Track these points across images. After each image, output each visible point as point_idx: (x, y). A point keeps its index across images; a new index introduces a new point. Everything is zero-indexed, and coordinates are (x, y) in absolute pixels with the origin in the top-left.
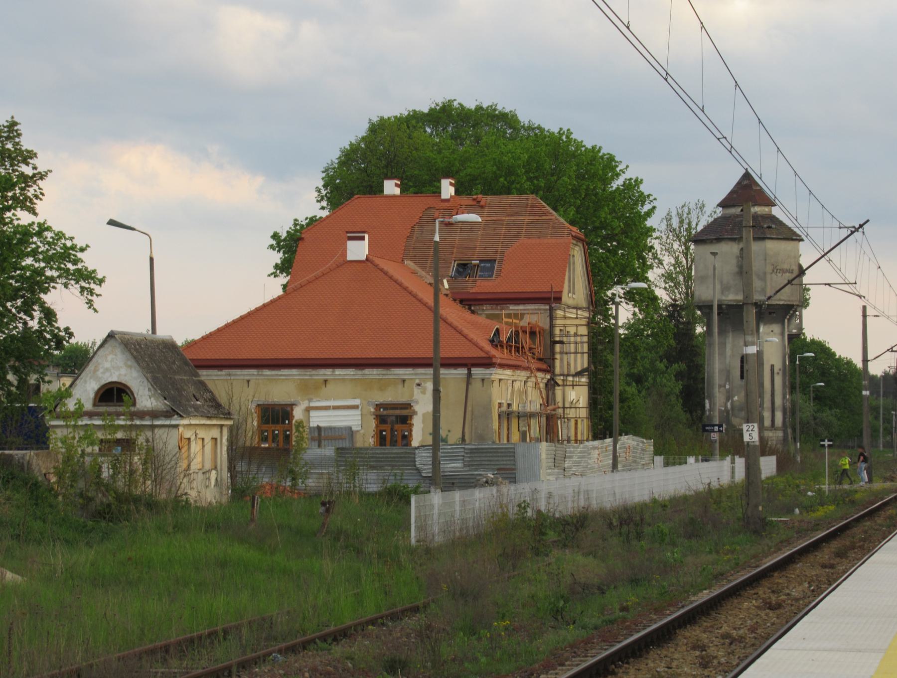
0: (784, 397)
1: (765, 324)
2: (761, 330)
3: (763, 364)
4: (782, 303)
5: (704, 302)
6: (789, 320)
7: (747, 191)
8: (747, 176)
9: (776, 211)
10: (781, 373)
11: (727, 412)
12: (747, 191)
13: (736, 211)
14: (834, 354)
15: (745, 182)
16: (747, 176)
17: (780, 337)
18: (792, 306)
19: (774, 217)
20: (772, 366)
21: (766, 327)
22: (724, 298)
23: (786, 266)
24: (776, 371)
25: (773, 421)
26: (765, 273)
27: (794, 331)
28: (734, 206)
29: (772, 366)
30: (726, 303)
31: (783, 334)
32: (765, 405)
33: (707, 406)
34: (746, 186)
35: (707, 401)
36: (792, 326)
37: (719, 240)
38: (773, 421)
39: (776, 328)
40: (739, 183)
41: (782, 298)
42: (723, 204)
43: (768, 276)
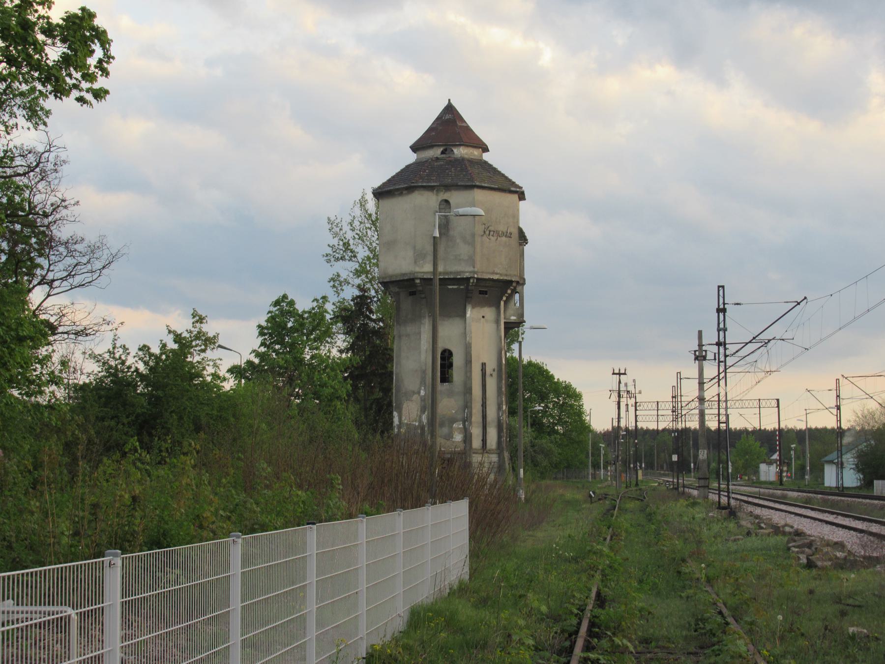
0: (499, 408)
1: (473, 308)
2: (468, 314)
3: (471, 361)
4: (496, 277)
5: (391, 276)
6: (506, 303)
7: (449, 129)
8: (450, 109)
9: (486, 157)
10: (495, 374)
11: (422, 428)
12: (449, 129)
13: (436, 152)
14: (552, 377)
15: (447, 117)
16: (450, 109)
17: (494, 326)
18: (511, 282)
19: (486, 162)
20: (484, 365)
21: (476, 310)
22: (417, 269)
23: (502, 228)
24: (489, 370)
25: (484, 441)
26: (473, 235)
27: (513, 318)
28: (431, 147)
29: (484, 365)
30: (420, 276)
31: (497, 322)
32: (473, 419)
33: (396, 421)
34: (448, 121)
35: (395, 414)
36: (510, 311)
37: (410, 189)
38: (484, 441)
39: (489, 312)
40: (438, 119)
41: (497, 270)
42: (415, 148)
43: (478, 239)
